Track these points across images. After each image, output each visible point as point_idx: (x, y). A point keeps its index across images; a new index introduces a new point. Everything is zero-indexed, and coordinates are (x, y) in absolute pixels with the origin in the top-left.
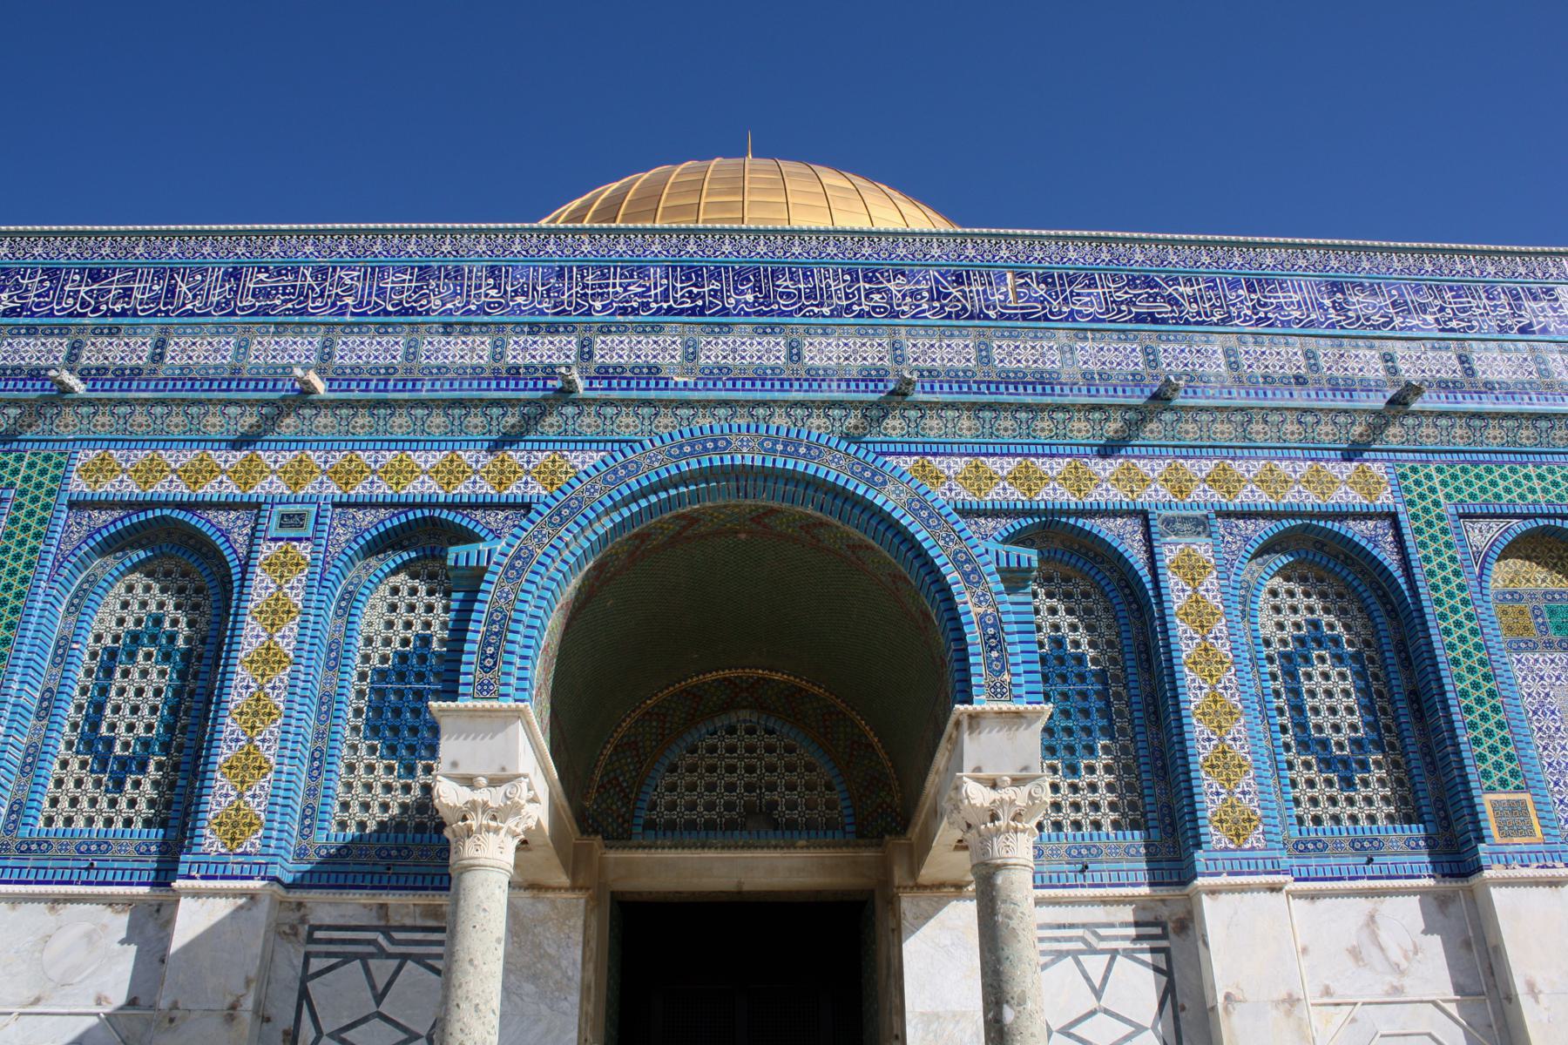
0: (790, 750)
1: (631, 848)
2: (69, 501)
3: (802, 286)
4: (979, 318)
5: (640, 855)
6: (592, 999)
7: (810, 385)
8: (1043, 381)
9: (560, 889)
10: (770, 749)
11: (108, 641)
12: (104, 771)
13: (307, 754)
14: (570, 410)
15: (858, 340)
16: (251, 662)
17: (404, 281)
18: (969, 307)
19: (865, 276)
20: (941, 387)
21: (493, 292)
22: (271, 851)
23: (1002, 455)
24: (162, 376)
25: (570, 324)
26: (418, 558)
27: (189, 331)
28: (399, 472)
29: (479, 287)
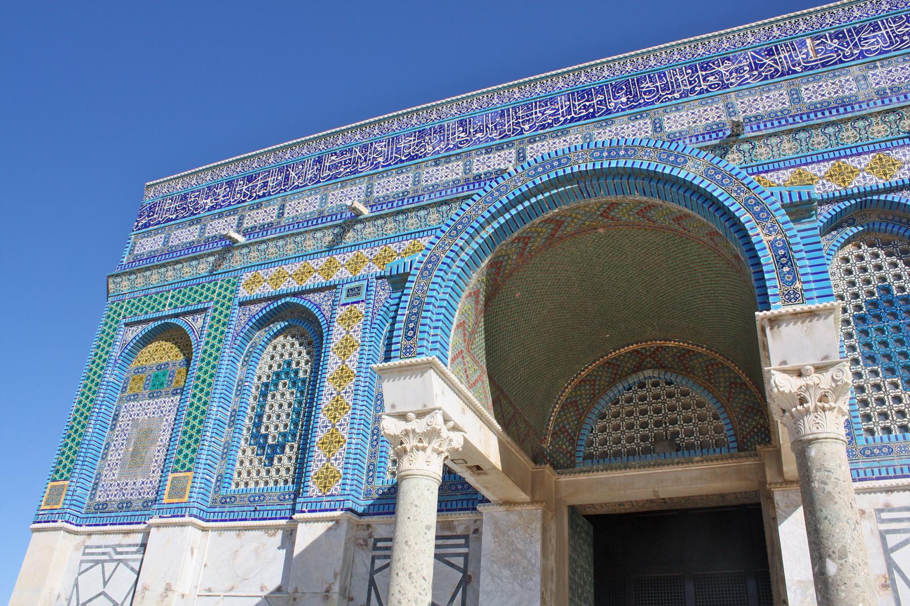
0: (685, 394)
1: (575, 473)
2: (239, 303)
3: (658, 84)
4: (788, 74)
5: (583, 477)
6: (555, 580)
8: (844, 104)
9: (523, 503)
10: (670, 395)
11: (264, 379)
12: (263, 454)
13: (370, 432)
16: (333, 379)
17: (411, 141)
18: (780, 69)
19: (702, 67)
20: (765, 126)
21: (463, 135)
22: (346, 492)
23: (819, 162)
24: (283, 224)
27: (296, 197)
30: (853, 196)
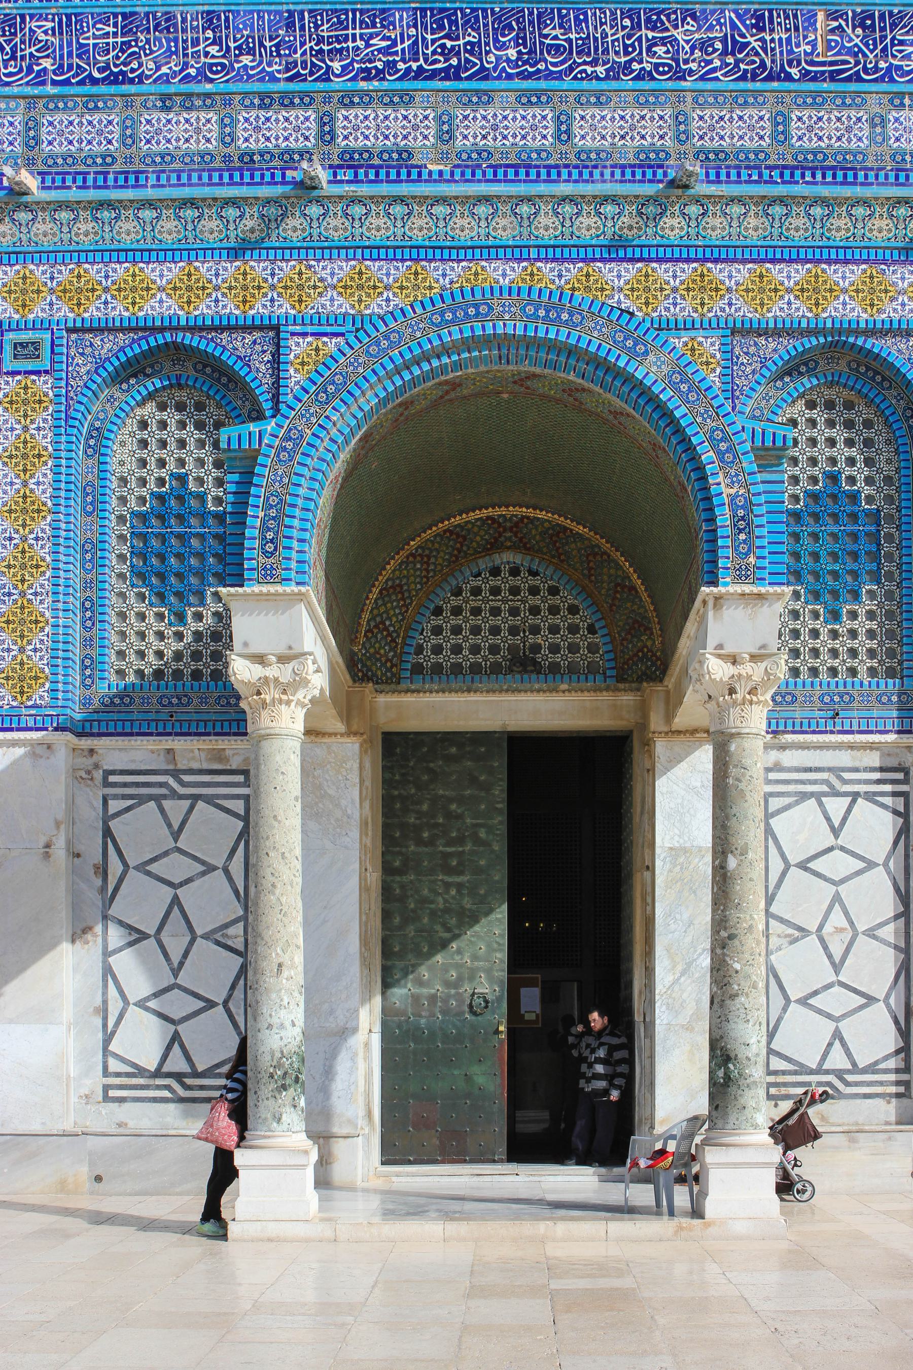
0: (554, 591)
1: (400, 692)
3: (573, 36)
4: (779, 79)
5: (409, 698)
6: (370, 833)
7: (581, 174)
9: (336, 734)
13: (78, 604)
14: (314, 210)
15: (636, 112)
19: (648, 20)
20: (728, 175)
21: (213, 50)
22: (60, 703)
25: (307, 93)
26: (164, 388)
28: (134, 289)
29: (196, 42)
30: (824, 332)
